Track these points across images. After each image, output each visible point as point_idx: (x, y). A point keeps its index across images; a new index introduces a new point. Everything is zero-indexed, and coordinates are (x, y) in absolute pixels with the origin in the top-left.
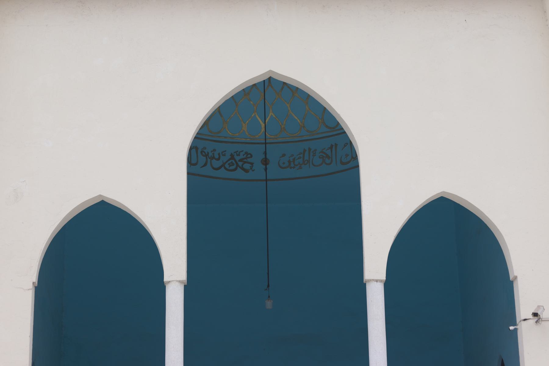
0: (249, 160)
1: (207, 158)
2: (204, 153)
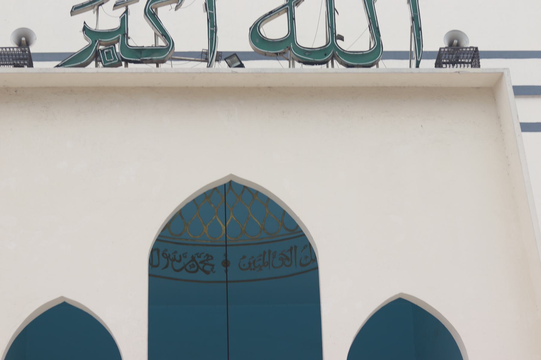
0: (210, 262)
1: (168, 260)
2: (165, 255)
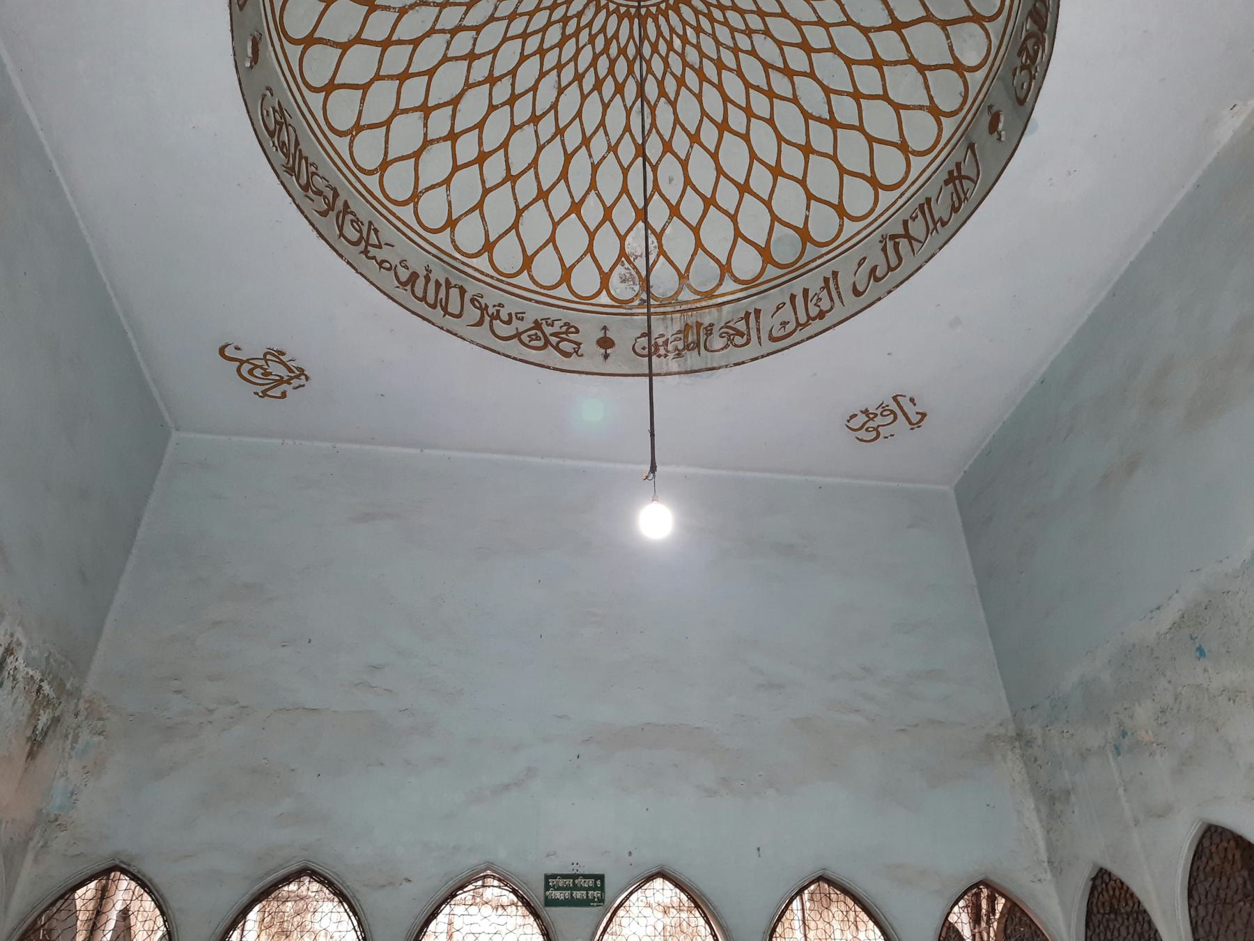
0: (572, 337)
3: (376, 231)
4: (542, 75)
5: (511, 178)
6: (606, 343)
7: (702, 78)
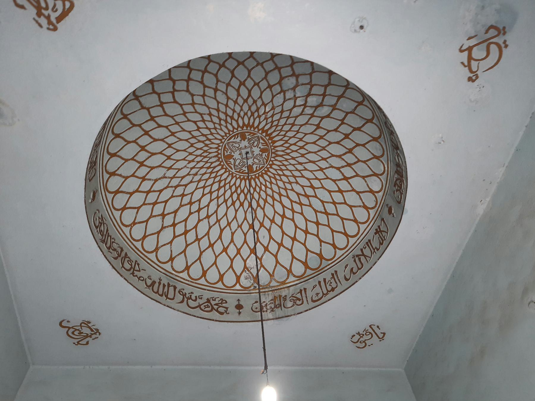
0: (224, 305)
3: (138, 264)
4: (211, 200)
5: (198, 240)
6: (239, 307)
7: (274, 199)
